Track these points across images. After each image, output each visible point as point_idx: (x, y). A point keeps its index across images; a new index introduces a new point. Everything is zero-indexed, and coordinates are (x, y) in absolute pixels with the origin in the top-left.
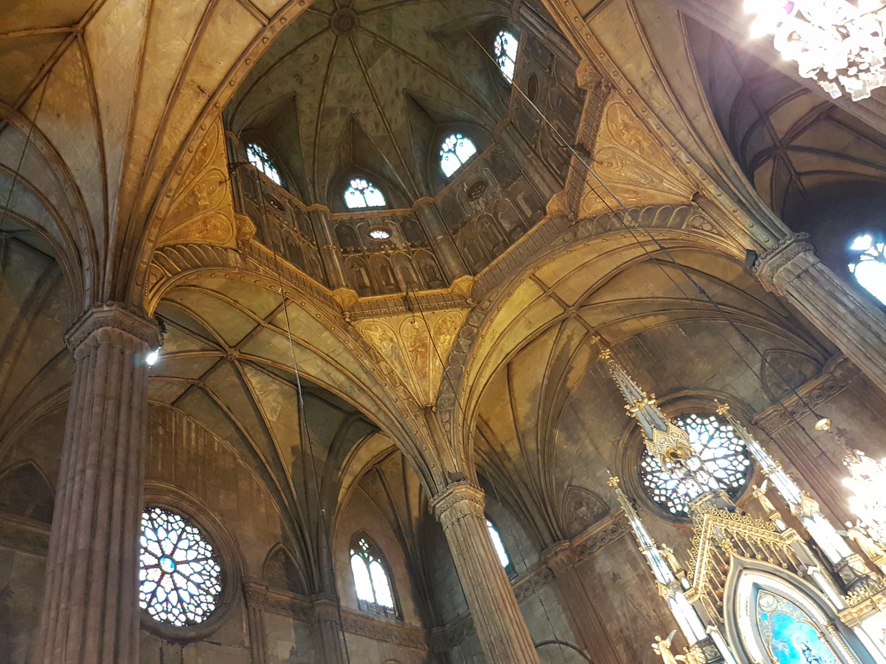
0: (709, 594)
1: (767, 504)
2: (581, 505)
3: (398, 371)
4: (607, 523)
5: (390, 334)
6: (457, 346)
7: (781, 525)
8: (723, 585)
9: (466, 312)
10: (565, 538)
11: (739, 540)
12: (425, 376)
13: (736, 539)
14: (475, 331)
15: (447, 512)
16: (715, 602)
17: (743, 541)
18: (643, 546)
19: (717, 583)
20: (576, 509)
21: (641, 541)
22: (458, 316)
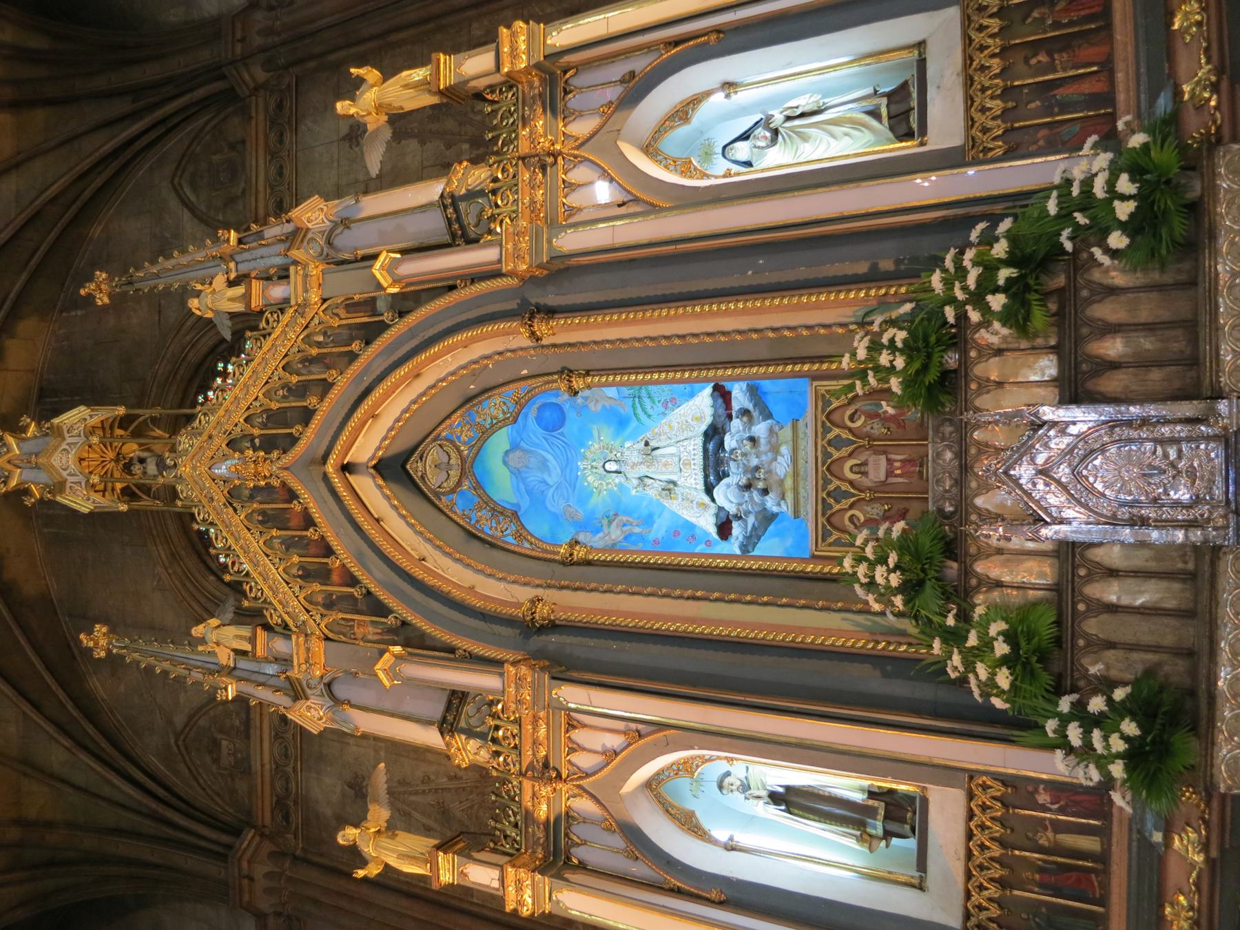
0: (330, 604)
2: (216, 744)
7: (278, 292)
8: (329, 551)
10: (237, 832)
11: (264, 426)
16: (351, 604)
20: (216, 760)
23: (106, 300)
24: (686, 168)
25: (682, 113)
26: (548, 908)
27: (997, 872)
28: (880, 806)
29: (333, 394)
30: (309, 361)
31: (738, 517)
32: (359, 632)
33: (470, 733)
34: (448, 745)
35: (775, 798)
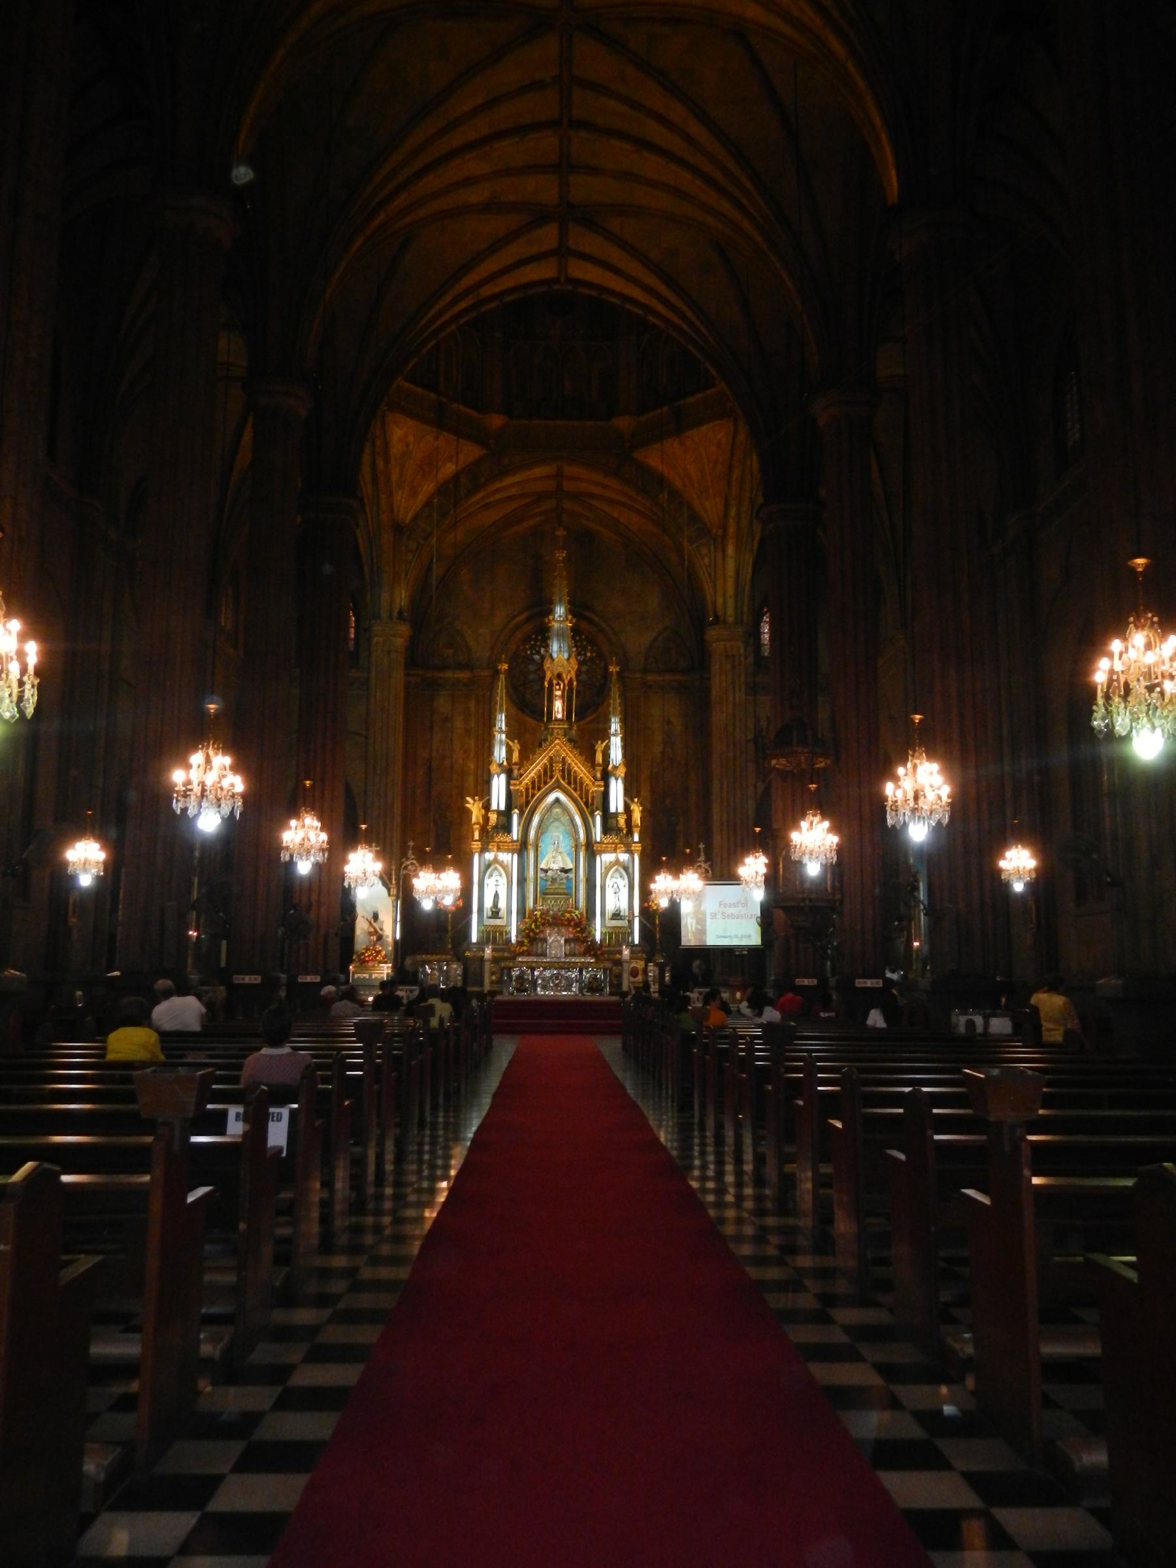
0: (527, 790)
1: (599, 758)
3: (394, 477)
4: (464, 675)
5: (411, 439)
6: (456, 478)
7: (599, 775)
8: (539, 789)
9: (484, 452)
12: (414, 493)
13: (566, 767)
14: (483, 480)
15: (381, 639)
16: (527, 796)
17: (569, 771)
18: (497, 728)
19: (536, 785)
21: (498, 725)
22: (471, 452)
23: (611, 670)
24: (612, 877)
25: (621, 877)
26: (474, 851)
27: (494, 930)
28: (497, 910)
29: (573, 792)
30: (581, 784)
31: (546, 876)
32: (521, 799)
33: (497, 819)
34: (493, 811)
35: (496, 892)
